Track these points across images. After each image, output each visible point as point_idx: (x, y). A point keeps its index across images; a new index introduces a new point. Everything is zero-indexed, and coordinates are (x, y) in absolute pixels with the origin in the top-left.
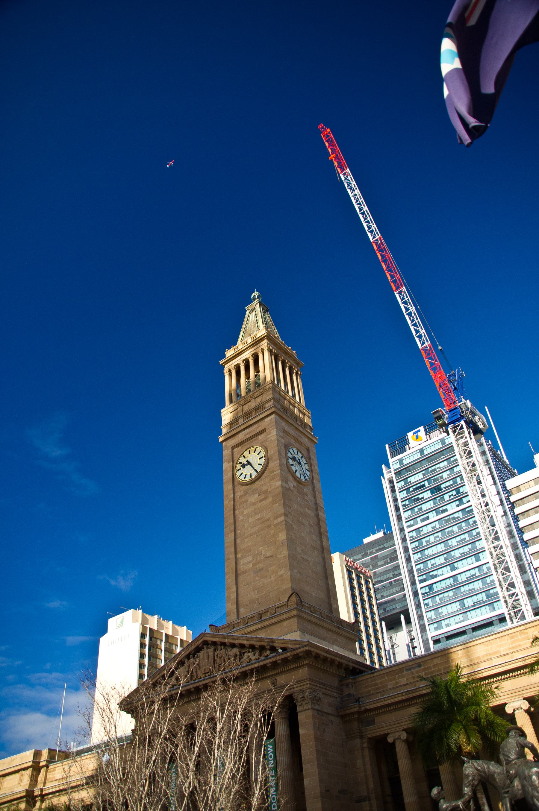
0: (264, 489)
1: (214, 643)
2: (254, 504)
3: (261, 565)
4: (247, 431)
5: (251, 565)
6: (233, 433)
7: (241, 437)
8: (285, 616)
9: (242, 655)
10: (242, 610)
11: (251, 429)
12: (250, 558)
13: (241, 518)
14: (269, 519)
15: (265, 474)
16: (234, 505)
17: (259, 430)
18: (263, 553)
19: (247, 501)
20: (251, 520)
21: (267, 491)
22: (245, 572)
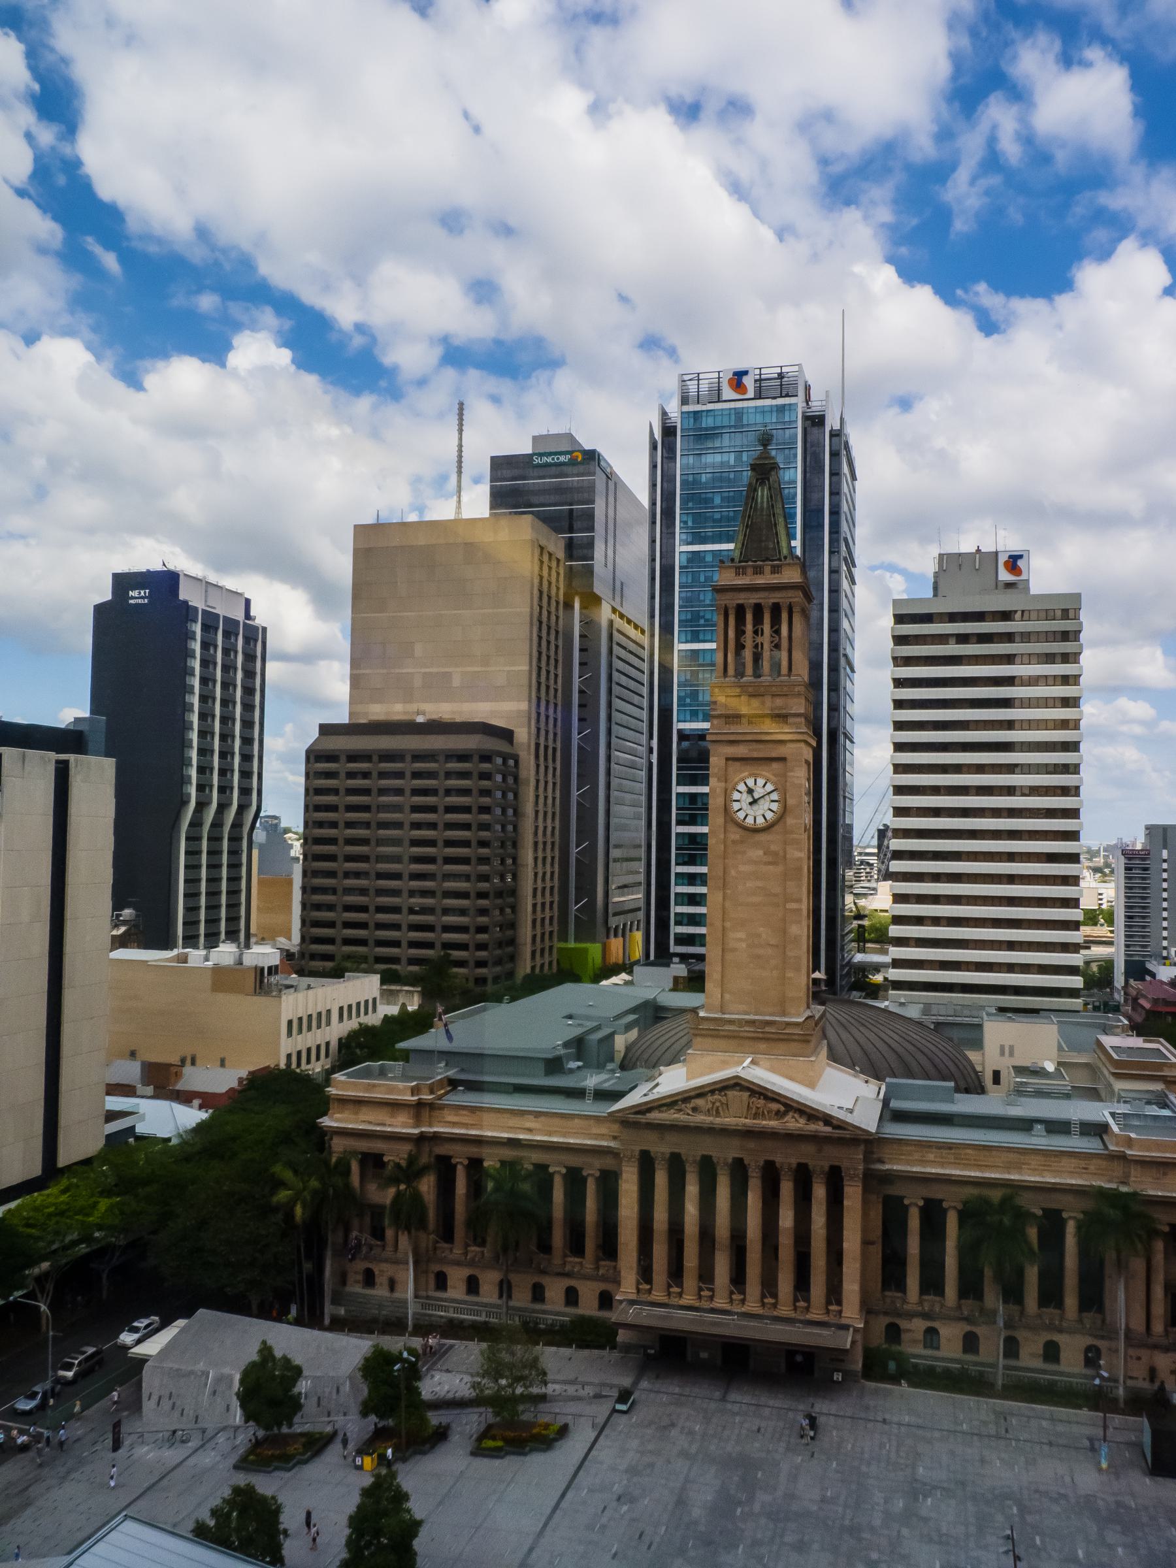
0: (773, 848)
1: (748, 1089)
2: (756, 863)
3: (761, 951)
4: (755, 746)
5: (744, 945)
6: (732, 738)
7: (741, 751)
8: (796, 1037)
9: (785, 1113)
10: (727, 996)
11: (761, 746)
12: (741, 935)
13: (733, 873)
14: (776, 895)
15: (776, 827)
16: (725, 851)
17: (774, 755)
18: (764, 936)
19: (744, 853)
20: (749, 884)
21: (776, 854)
22: (734, 950)
